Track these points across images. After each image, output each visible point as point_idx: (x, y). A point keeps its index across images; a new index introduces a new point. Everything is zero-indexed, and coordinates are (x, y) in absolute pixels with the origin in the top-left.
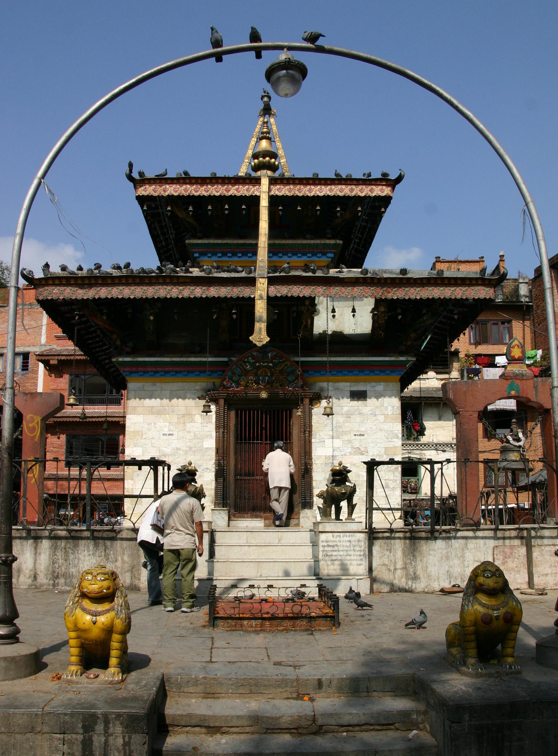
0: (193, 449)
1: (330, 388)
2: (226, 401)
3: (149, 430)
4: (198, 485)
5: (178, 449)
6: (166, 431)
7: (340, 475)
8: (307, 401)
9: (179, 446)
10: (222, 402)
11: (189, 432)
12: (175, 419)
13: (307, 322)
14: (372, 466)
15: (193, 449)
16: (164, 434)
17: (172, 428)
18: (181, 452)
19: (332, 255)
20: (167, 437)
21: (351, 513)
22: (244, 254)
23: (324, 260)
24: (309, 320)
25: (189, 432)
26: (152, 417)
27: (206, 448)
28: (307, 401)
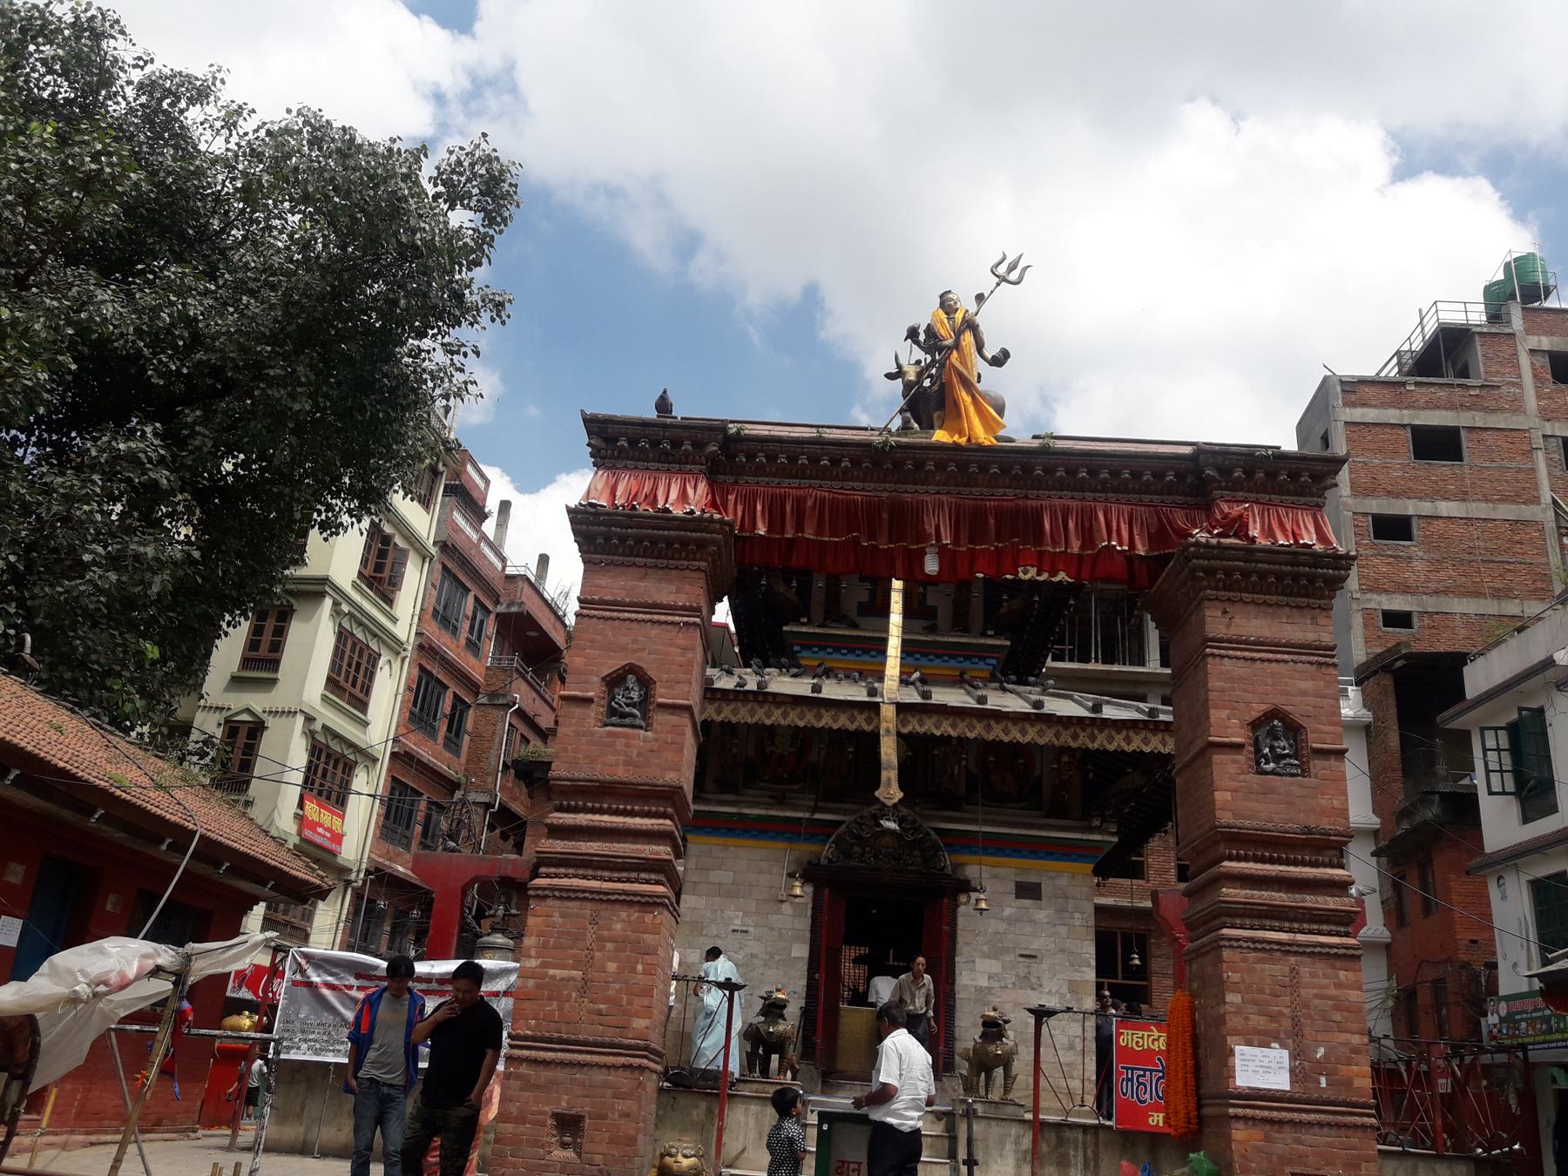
1: (985, 875)
3: (712, 921)
5: (753, 956)
9: (754, 951)
11: (772, 929)
12: (752, 906)
14: (1041, 1015)
15: (777, 958)
17: (748, 921)
19: (994, 662)
20: (739, 935)
21: (1007, 1089)
22: (866, 651)
23: (983, 668)
25: (772, 929)
26: (717, 899)
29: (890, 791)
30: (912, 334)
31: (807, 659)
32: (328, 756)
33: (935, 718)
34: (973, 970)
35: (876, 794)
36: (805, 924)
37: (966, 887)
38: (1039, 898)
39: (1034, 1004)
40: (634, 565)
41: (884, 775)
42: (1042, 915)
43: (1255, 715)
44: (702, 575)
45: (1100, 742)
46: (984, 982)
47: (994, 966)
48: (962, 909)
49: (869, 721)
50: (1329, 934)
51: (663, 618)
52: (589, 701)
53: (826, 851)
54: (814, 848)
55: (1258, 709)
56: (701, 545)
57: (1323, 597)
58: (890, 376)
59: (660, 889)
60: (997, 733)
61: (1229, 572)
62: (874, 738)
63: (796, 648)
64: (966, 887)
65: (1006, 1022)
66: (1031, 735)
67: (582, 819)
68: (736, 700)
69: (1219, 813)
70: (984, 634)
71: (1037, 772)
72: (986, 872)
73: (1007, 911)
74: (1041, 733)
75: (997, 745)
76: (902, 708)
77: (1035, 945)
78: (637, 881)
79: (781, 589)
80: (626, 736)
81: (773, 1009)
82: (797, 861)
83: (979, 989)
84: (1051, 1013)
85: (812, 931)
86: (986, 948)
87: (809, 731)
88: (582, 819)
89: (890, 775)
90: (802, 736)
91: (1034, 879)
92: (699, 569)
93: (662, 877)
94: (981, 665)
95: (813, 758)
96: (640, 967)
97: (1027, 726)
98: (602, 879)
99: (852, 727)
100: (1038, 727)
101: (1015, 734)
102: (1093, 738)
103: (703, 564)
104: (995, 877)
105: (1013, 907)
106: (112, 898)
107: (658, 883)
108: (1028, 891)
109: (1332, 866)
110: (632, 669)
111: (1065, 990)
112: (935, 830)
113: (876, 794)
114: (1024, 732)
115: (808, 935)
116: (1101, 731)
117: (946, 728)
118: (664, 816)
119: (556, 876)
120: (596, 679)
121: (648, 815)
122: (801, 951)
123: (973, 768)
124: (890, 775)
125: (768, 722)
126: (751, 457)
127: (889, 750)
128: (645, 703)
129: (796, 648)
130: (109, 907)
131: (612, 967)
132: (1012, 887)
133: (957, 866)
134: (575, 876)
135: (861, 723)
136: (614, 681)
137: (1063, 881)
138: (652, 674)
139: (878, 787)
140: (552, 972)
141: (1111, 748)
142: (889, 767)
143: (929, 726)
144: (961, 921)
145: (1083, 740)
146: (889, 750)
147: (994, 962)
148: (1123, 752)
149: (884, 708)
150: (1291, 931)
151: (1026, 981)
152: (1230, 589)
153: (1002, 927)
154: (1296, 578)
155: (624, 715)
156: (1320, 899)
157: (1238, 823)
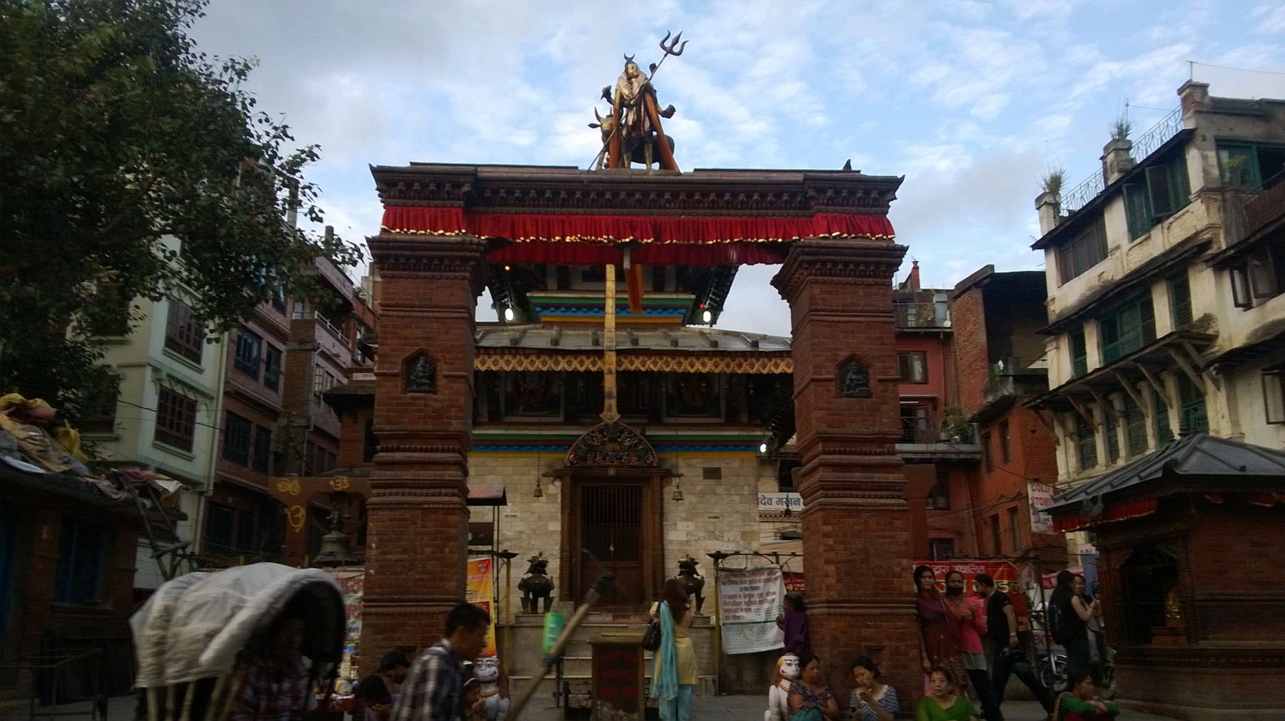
2: (572, 478)
4: (548, 577)
5: (522, 532)
7: (688, 567)
8: (657, 480)
10: (567, 479)
28: (657, 480)
29: (611, 413)
31: (546, 316)
32: (174, 402)
33: (641, 358)
34: (675, 529)
40: (417, 277)
41: (607, 402)
42: (720, 490)
43: (841, 359)
44: (466, 282)
45: (757, 368)
46: (683, 538)
47: (691, 526)
50: (887, 497)
52: (396, 375)
53: (568, 456)
54: (562, 456)
55: (843, 355)
56: (464, 260)
57: (885, 277)
59: (455, 499)
60: (686, 366)
61: (824, 263)
62: (600, 375)
63: (538, 309)
64: (668, 475)
66: (707, 367)
67: (399, 456)
68: (495, 353)
70: (677, 291)
71: (716, 390)
72: (681, 462)
73: (698, 488)
74: (716, 365)
75: (686, 375)
76: (619, 353)
77: (717, 510)
78: (439, 495)
80: (424, 398)
81: (538, 566)
82: (549, 466)
83: (681, 543)
84: (725, 556)
87: (550, 373)
88: (399, 456)
89: (611, 403)
90: (547, 377)
91: (716, 465)
92: (464, 278)
93: (456, 491)
94: (675, 315)
95: (555, 390)
96: (447, 550)
97: (706, 360)
98: (415, 495)
99: (582, 369)
100: (714, 360)
101: (698, 367)
102: (752, 366)
103: (467, 274)
104: (689, 466)
105: (702, 484)
106: (46, 528)
107: (453, 495)
108: (712, 474)
109: (889, 453)
110: (422, 353)
111: (739, 538)
114: (704, 365)
117: (650, 365)
118: (453, 451)
119: (384, 495)
120: (400, 361)
121: (443, 451)
124: (611, 403)
125: (520, 369)
126: (495, 192)
127: (610, 383)
128: (432, 377)
130: (45, 536)
131: (428, 550)
133: (661, 461)
134: (397, 494)
135: (588, 365)
136: (411, 361)
137: (736, 464)
138: (439, 355)
139: (602, 410)
140: (388, 557)
141: (765, 372)
142: (610, 396)
143: (637, 364)
145: (746, 368)
146: (610, 383)
147: (690, 524)
150: (863, 497)
151: (712, 535)
152: (825, 275)
153: (694, 499)
154: (867, 264)
155: (419, 385)
156: (883, 475)
157: (829, 430)
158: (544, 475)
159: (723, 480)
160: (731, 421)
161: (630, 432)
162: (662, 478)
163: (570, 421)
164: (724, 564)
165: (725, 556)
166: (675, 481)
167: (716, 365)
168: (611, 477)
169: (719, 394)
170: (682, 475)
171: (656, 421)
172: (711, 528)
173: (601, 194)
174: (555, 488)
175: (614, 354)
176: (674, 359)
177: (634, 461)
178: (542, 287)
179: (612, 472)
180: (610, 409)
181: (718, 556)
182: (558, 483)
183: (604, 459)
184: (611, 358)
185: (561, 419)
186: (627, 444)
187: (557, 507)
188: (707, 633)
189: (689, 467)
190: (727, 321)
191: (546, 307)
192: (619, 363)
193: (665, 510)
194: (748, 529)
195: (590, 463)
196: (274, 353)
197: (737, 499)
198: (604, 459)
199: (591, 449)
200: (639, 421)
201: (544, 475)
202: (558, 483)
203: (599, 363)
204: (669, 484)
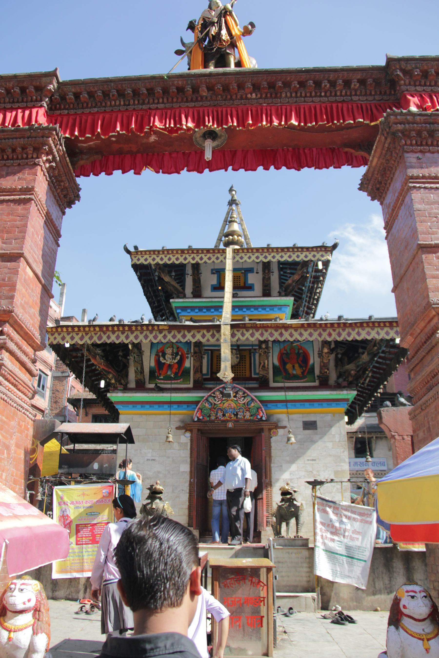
0: (171, 472)
2: (198, 430)
5: (159, 472)
6: (149, 456)
10: (195, 431)
13: (264, 363)
15: (171, 472)
16: (148, 460)
18: (161, 475)
24: (266, 361)
25: (168, 457)
27: (182, 472)
30: (191, 26)
35: (218, 375)
36: (187, 453)
37: (277, 426)
38: (316, 429)
39: (312, 480)
48: (273, 439)
49: (213, 336)
51: (7, 198)
54: (191, 412)
58: (179, 53)
63: (179, 311)
65: (295, 492)
69: (431, 294)
71: (311, 362)
79: (167, 279)
82: (182, 421)
84: (321, 483)
85: (191, 457)
86: (288, 458)
91: (312, 418)
95: (188, 364)
97: (302, 331)
101: (296, 336)
108: (310, 425)
112: (255, 396)
113: (218, 375)
115: (189, 460)
116: (344, 330)
122: (186, 468)
123: (276, 363)
129: (179, 311)
132: (301, 424)
133: (269, 417)
139: (219, 370)
141: (350, 339)
142: (226, 360)
144: (273, 444)
148: (357, 341)
149: (223, 327)
158: (177, 428)
159: (319, 430)
160: (324, 384)
161: (244, 393)
162: (270, 430)
163: (198, 386)
164: (321, 491)
165: (321, 483)
166: (281, 432)
167: (311, 335)
168: (230, 429)
169: (313, 365)
170: (284, 427)
171: (264, 385)
172: (310, 469)
173: (180, 90)
174: (185, 438)
175: (229, 327)
176: (276, 331)
177: (248, 416)
178: (181, 295)
179: (230, 425)
180: (226, 370)
181: (315, 484)
182: (188, 434)
183: (224, 415)
184: (226, 331)
185: (191, 385)
186: (242, 401)
187: (186, 454)
188: (305, 553)
189: (290, 421)
190: (317, 317)
191: (184, 309)
192: (233, 335)
193: (273, 454)
194: (339, 469)
195: (213, 418)
196: (43, 375)
197: (330, 445)
198: (224, 415)
199: (214, 407)
200: (251, 386)
201: (177, 428)
202: (188, 434)
203: (217, 336)
204: (276, 434)
